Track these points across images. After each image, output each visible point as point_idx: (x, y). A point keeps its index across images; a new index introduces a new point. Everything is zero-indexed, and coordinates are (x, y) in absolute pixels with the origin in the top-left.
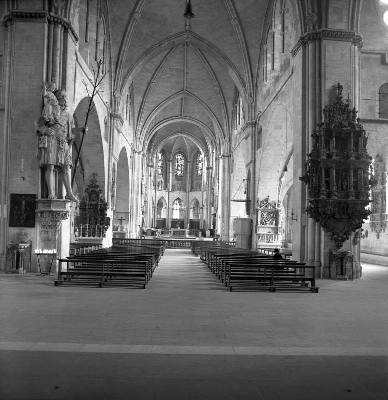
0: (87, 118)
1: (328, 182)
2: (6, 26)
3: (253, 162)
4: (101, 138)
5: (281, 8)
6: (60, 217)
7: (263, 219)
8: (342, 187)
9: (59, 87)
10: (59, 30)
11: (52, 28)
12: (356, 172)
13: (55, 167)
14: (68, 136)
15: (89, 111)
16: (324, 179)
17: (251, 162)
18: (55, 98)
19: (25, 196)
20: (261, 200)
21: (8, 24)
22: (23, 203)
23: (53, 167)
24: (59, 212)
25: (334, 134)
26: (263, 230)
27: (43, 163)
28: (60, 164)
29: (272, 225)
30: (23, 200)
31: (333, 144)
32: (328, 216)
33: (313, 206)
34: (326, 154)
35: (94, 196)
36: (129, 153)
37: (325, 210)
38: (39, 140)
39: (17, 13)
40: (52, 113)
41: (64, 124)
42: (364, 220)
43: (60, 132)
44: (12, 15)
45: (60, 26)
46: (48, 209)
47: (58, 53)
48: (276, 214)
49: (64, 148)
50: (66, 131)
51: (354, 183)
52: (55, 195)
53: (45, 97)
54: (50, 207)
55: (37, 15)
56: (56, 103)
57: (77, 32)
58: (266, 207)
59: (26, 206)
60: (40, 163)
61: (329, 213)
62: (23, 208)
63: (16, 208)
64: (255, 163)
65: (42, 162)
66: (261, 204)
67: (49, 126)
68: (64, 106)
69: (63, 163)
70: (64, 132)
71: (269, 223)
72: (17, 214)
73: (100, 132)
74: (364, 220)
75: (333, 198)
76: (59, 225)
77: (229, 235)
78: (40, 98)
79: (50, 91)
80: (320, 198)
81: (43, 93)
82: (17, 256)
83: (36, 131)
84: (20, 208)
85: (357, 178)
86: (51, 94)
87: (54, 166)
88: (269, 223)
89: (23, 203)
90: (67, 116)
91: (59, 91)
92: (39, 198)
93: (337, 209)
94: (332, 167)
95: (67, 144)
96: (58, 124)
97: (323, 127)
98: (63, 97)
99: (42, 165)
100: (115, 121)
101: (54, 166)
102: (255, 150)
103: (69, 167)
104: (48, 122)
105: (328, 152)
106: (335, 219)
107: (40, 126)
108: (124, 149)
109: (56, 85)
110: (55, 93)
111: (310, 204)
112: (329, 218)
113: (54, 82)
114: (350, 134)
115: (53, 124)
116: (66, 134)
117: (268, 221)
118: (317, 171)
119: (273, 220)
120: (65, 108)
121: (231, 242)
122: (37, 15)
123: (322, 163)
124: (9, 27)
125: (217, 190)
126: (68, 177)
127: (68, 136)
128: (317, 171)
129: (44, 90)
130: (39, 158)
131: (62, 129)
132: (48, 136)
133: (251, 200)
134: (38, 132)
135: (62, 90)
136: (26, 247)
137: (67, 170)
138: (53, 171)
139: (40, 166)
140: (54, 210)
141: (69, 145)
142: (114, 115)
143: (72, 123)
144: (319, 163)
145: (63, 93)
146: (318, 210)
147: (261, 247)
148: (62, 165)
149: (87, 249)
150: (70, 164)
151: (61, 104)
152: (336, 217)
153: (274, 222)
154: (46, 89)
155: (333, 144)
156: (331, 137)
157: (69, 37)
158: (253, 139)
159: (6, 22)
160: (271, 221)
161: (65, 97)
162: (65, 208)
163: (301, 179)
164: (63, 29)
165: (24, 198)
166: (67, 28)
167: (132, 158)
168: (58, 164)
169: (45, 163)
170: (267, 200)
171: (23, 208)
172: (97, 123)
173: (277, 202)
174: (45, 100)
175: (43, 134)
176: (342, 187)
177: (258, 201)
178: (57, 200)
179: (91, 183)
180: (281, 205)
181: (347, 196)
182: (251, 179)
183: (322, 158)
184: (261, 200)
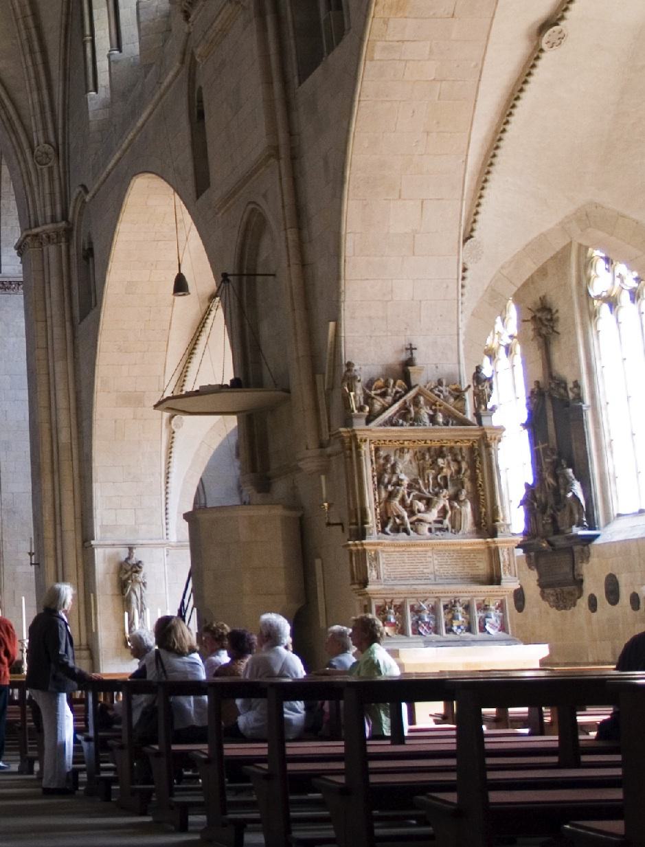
7: (391, 495)
17: (274, 152)
29: (456, 527)
58: (404, 414)
64: (294, 157)
66: (368, 399)
71: (433, 515)
88: (433, 515)
102: (285, 82)
117: (429, 504)
119: (455, 497)
153: (467, 509)
158: (270, 19)
160: (443, 502)
170: (404, 370)
173: (467, 380)
177: (350, 379)
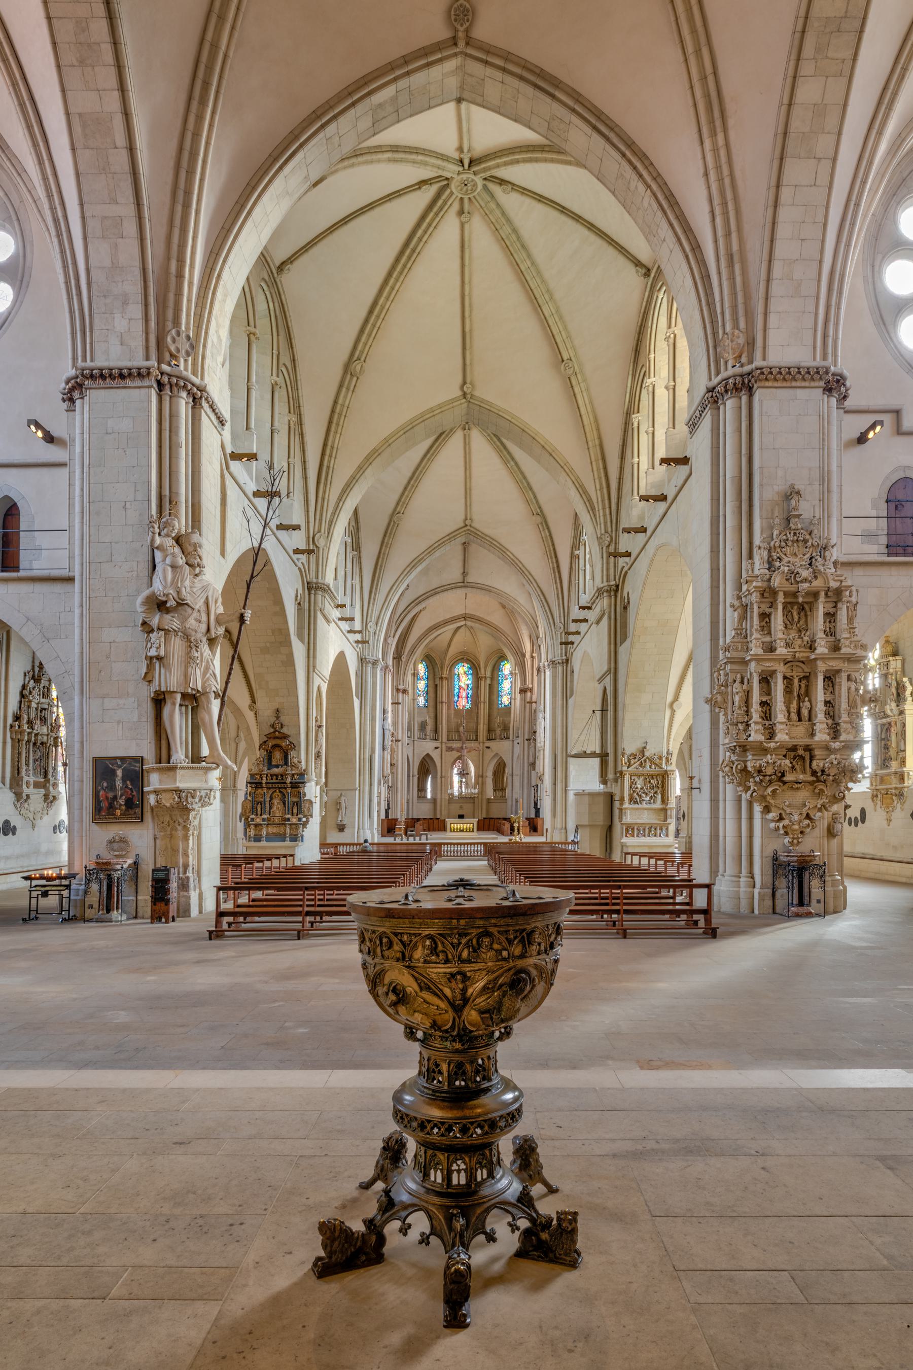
0: (248, 591)
1: (768, 705)
2: (72, 400)
3: (613, 670)
4: (289, 635)
5: (669, 327)
6: (197, 800)
8: (799, 713)
9: (187, 527)
10: (183, 403)
11: (166, 399)
12: (830, 679)
13: (184, 696)
14: (208, 630)
15: (252, 577)
16: (756, 697)
18: (177, 550)
19: (123, 759)
20: (628, 752)
21: (76, 394)
22: (119, 773)
23: (179, 696)
24: (194, 790)
25: (781, 598)
26: (632, 815)
27: (157, 688)
28: (193, 689)
30: (119, 767)
31: (778, 620)
32: (768, 778)
33: (734, 758)
34: (763, 642)
35: (277, 756)
36: (352, 665)
37: (760, 765)
38: (148, 640)
39: (92, 370)
40: (172, 584)
41: (200, 604)
42: (850, 785)
43: (191, 622)
44: (83, 375)
45: (184, 394)
46: (172, 786)
47: (183, 451)
48: (663, 778)
49: (202, 655)
50: (204, 618)
51: (827, 703)
52: (187, 756)
53: (157, 548)
54: (175, 780)
55: (134, 371)
56: (181, 561)
57: (225, 411)
59: (124, 780)
60: (152, 689)
61: (769, 771)
62: (119, 783)
63: (105, 784)
65: (155, 687)
67: (168, 611)
68: (199, 565)
69: (200, 689)
70: (200, 622)
72: (107, 798)
73: (286, 622)
74: (850, 785)
75: (777, 739)
76: (195, 818)
77: (566, 829)
78: (146, 550)
79: (167, 535)
80: (750, 739)
81: (153, 540)
82: (108, 884)
83: (141, 621)
84: (112, 787)
85: (832, 693)
86: (170, 542)
87: (182, 693)
89: (119, 773)
90: (205, 588)
91: (187, 534)
92: (150, 763)
93: (787, 762)
94: (774, 672)
95: (206, 646)
96: (186, 604)
97: (755, 583)
98: (196, 546)
99: (155, 692)
100: (319, 597)
101: (182, 693)
103: (213, 695)
104: (166, 602)
105: (768, 639)
106: (785, 783)
107: (148, 611)
108: (341, 657)
109: (181, 524)
110: (178, 540)
111: (728, 754)
112: (770, 782)
113: (176, 516)
114: (816, 595)
115: (173, 603)
116: (204, 627)
118: (742, 682)
120: (201, 571)
121: (569, 843)
122: (134, 371)
123: (753, 665)
124: (78, 403)
125: (542, 735)
126: (209, 713)
127: (208, 630)
128: (742, 682)
129: (154, 533)
130: (148, 678)
131: (195, 614)
132: (167, 632)
133: (609, 751)
134: (144, 623)
135: (193, 532)
136: (125, 866)
137: (209, 702)
138: (181, 705)
139: (152, 695)
140: (181, 785)
141: (211, 649)
142: (316, 583)
143: (216, 602)
144: (745, 663)
145: (195, 538)
146: (746, 767)
147: (630, 851)
148: (198, 691)
149: (260, 865)
150: (214, 689)
151: (192, 561)
152: (785, 779)
154: (157, 530)
155: (778, 620)
156: (772, 605)
157: (204, 417)
159: (72, 390)
161: (200, 546)
162: (206, 781)
163: (707, 701)
164: (191, 400)
165: (119, 763)
166: (198, 397)
167: (361, 675)
168: (190, 691)
169: (163, 689)
171: (119, 783)
172: (278, 601)
174: (158, 555)
175: (155, 626)
176: (799, 713)
178: (190, 765)
179: (272, 730)
180: (674, 759)
181: (813, 735)
182: (609, 709)
183: (752, 652)
184: (628, 752)
